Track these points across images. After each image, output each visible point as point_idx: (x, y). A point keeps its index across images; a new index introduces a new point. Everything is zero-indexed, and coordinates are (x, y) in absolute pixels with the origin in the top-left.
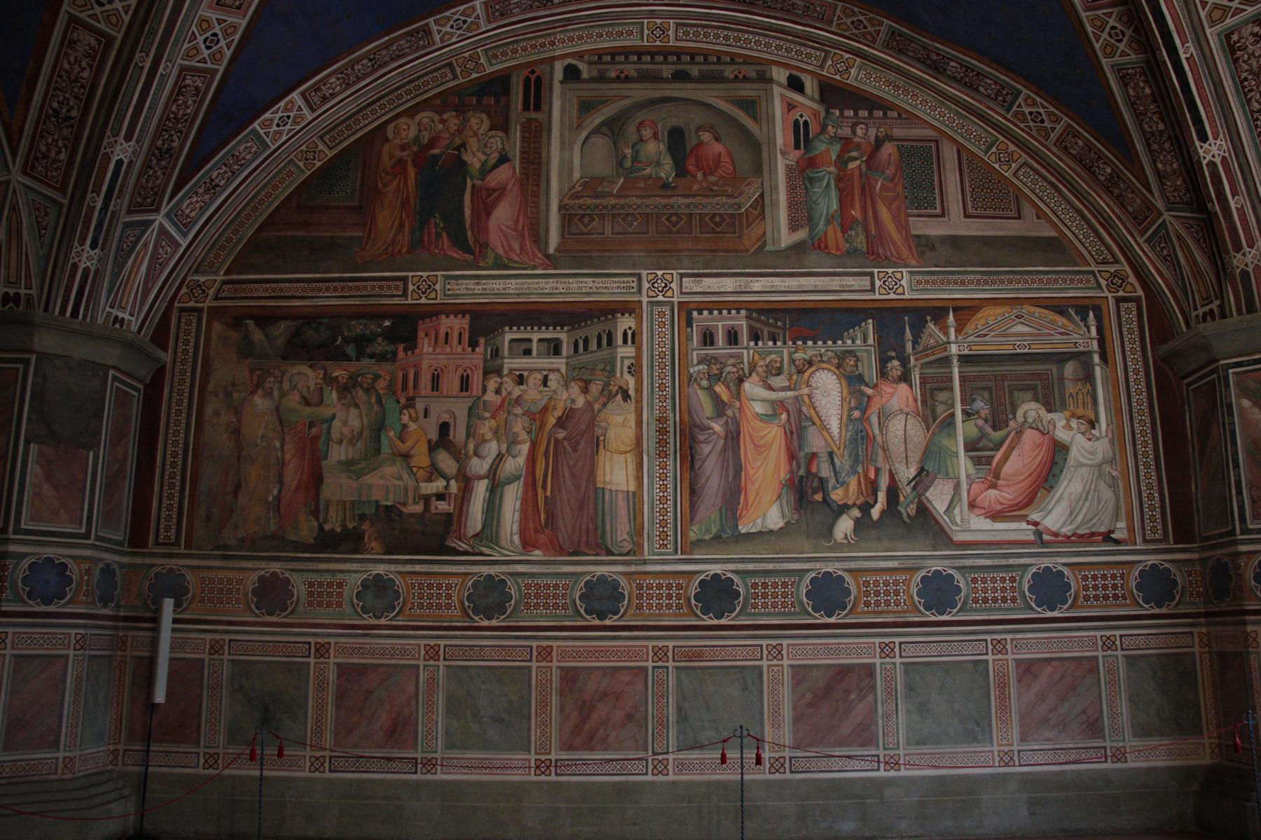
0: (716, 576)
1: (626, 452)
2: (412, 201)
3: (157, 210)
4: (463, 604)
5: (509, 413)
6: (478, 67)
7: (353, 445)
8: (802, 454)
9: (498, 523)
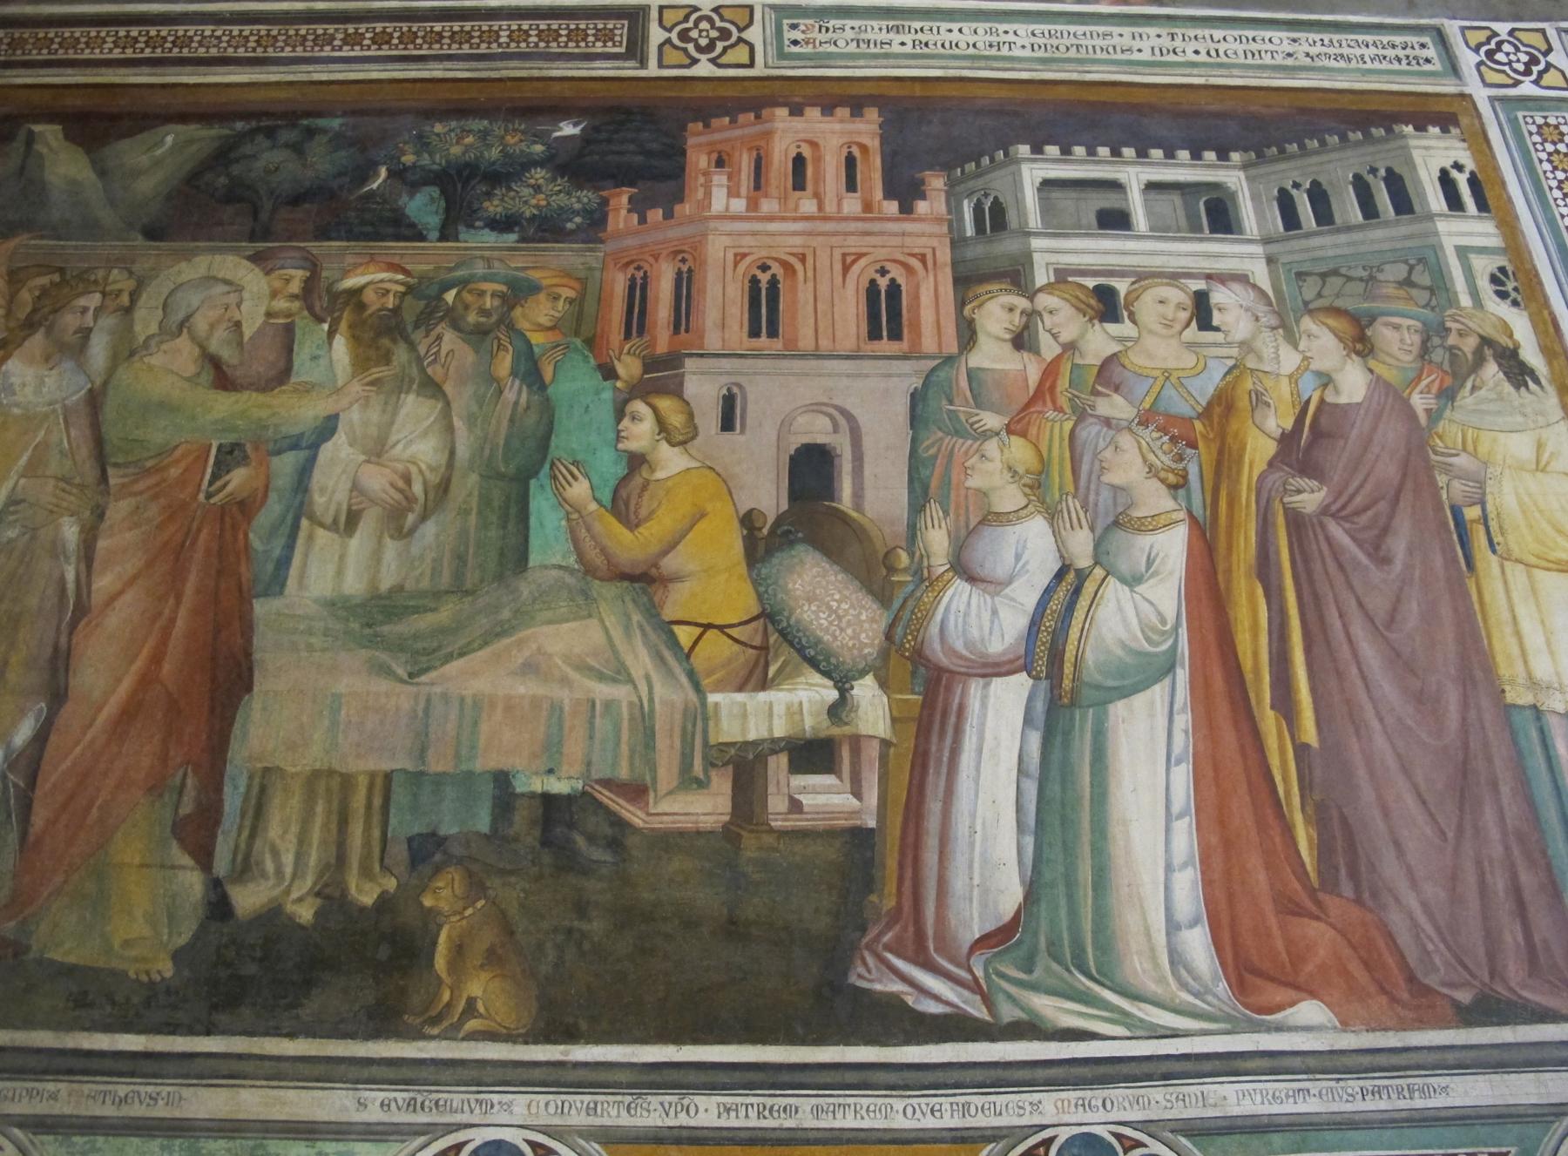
5: (1081, 415)
7: (403, 534)
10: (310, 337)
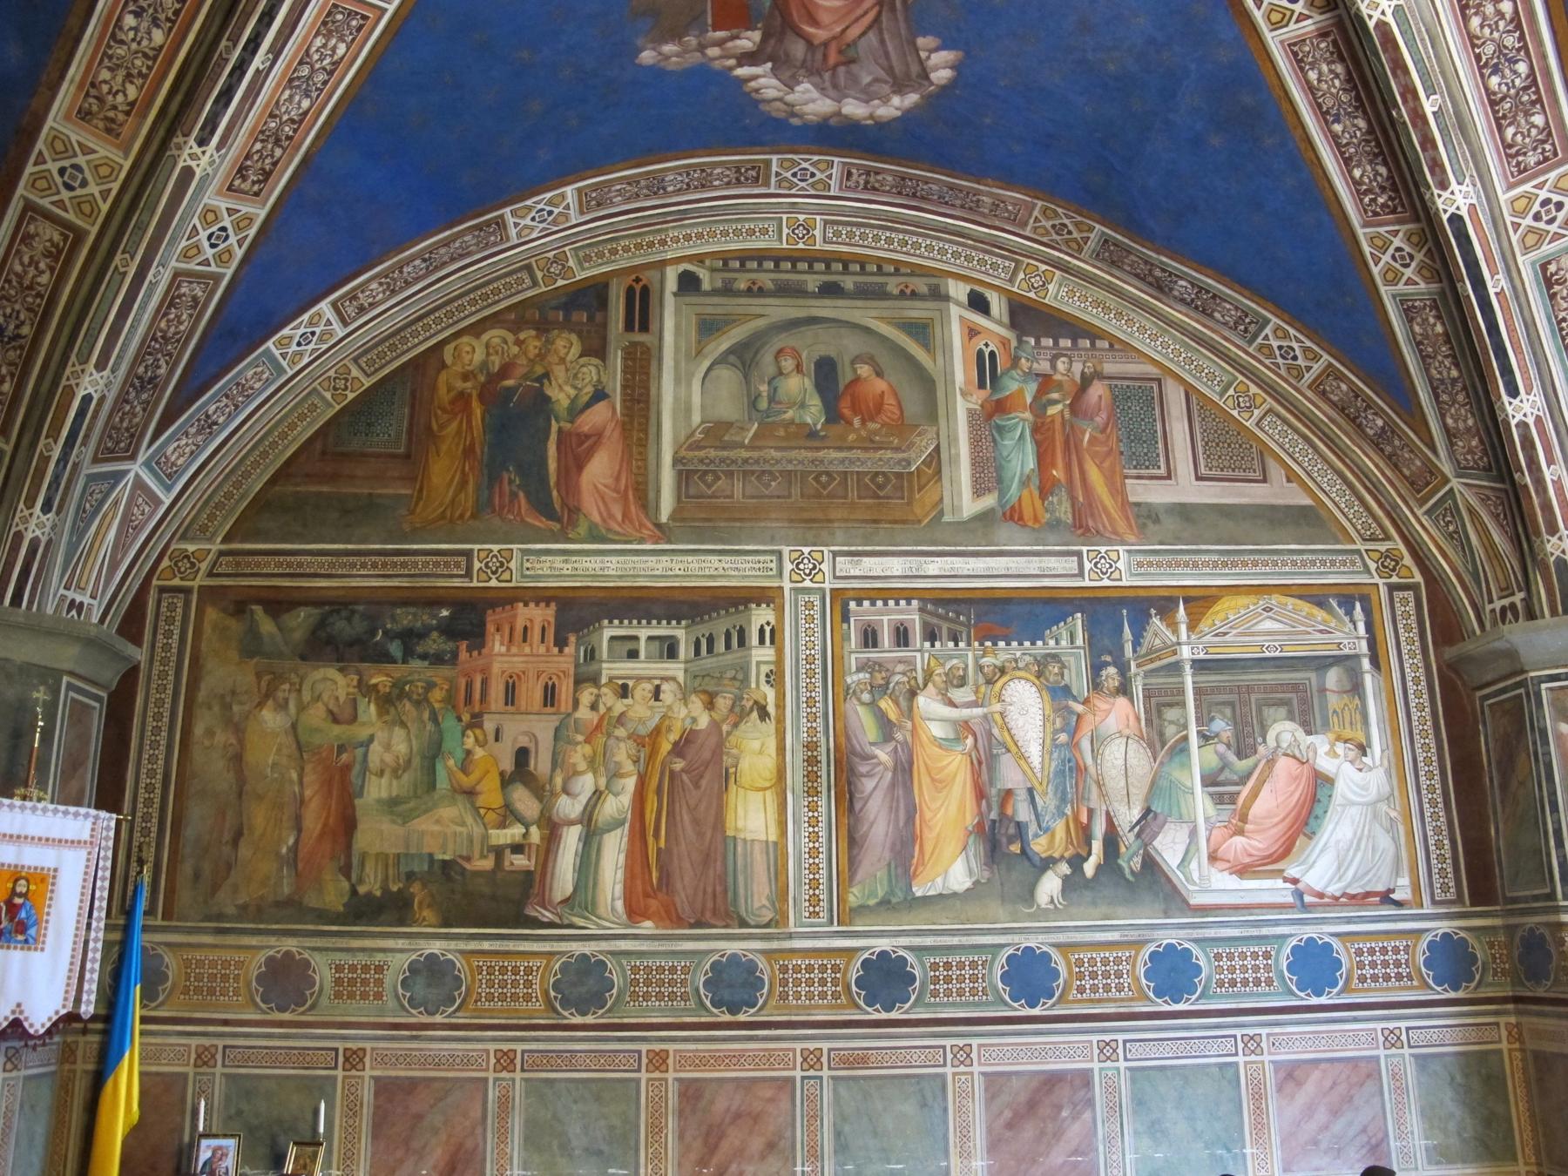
0: (883, 954)
1: (765, 789)
2: (478, 450)
3: (133, 457)
4: (546, 993)
5: (609, 735)
6: (566, 271)
7: (398, 777)
8: (994, 791)
9: (595, 884)
10: (362, 703)
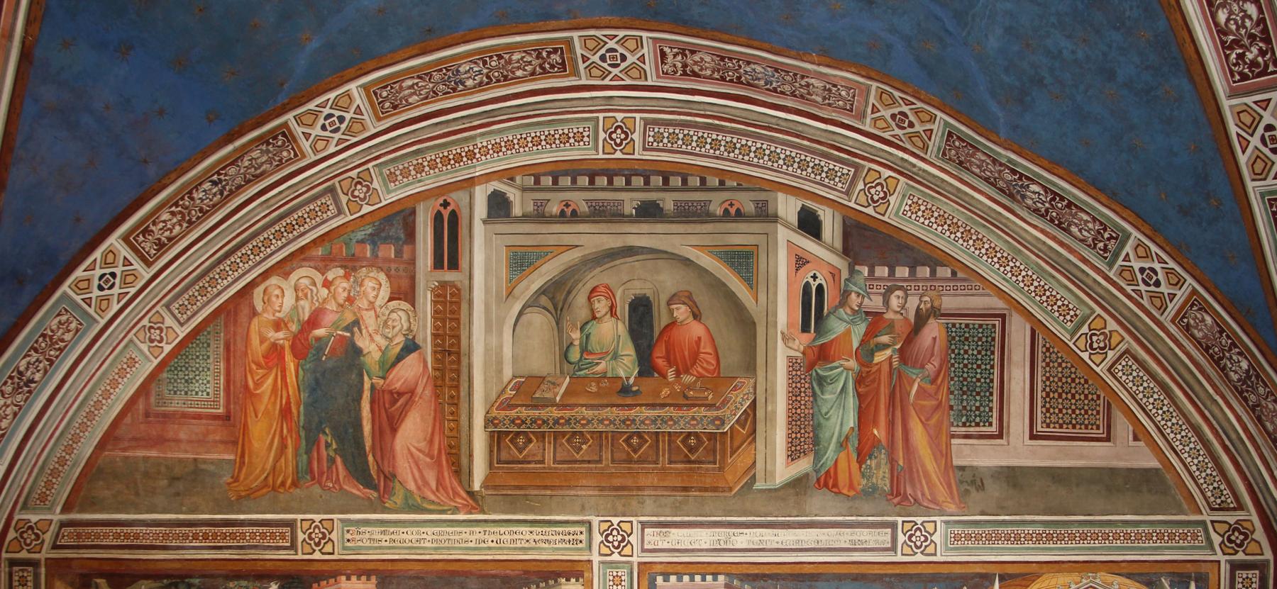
2: (294, 410)
